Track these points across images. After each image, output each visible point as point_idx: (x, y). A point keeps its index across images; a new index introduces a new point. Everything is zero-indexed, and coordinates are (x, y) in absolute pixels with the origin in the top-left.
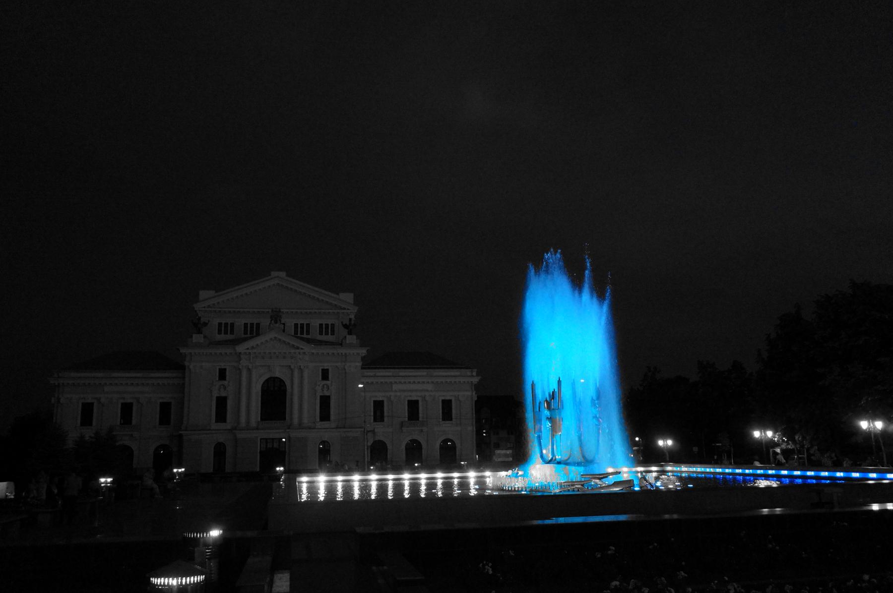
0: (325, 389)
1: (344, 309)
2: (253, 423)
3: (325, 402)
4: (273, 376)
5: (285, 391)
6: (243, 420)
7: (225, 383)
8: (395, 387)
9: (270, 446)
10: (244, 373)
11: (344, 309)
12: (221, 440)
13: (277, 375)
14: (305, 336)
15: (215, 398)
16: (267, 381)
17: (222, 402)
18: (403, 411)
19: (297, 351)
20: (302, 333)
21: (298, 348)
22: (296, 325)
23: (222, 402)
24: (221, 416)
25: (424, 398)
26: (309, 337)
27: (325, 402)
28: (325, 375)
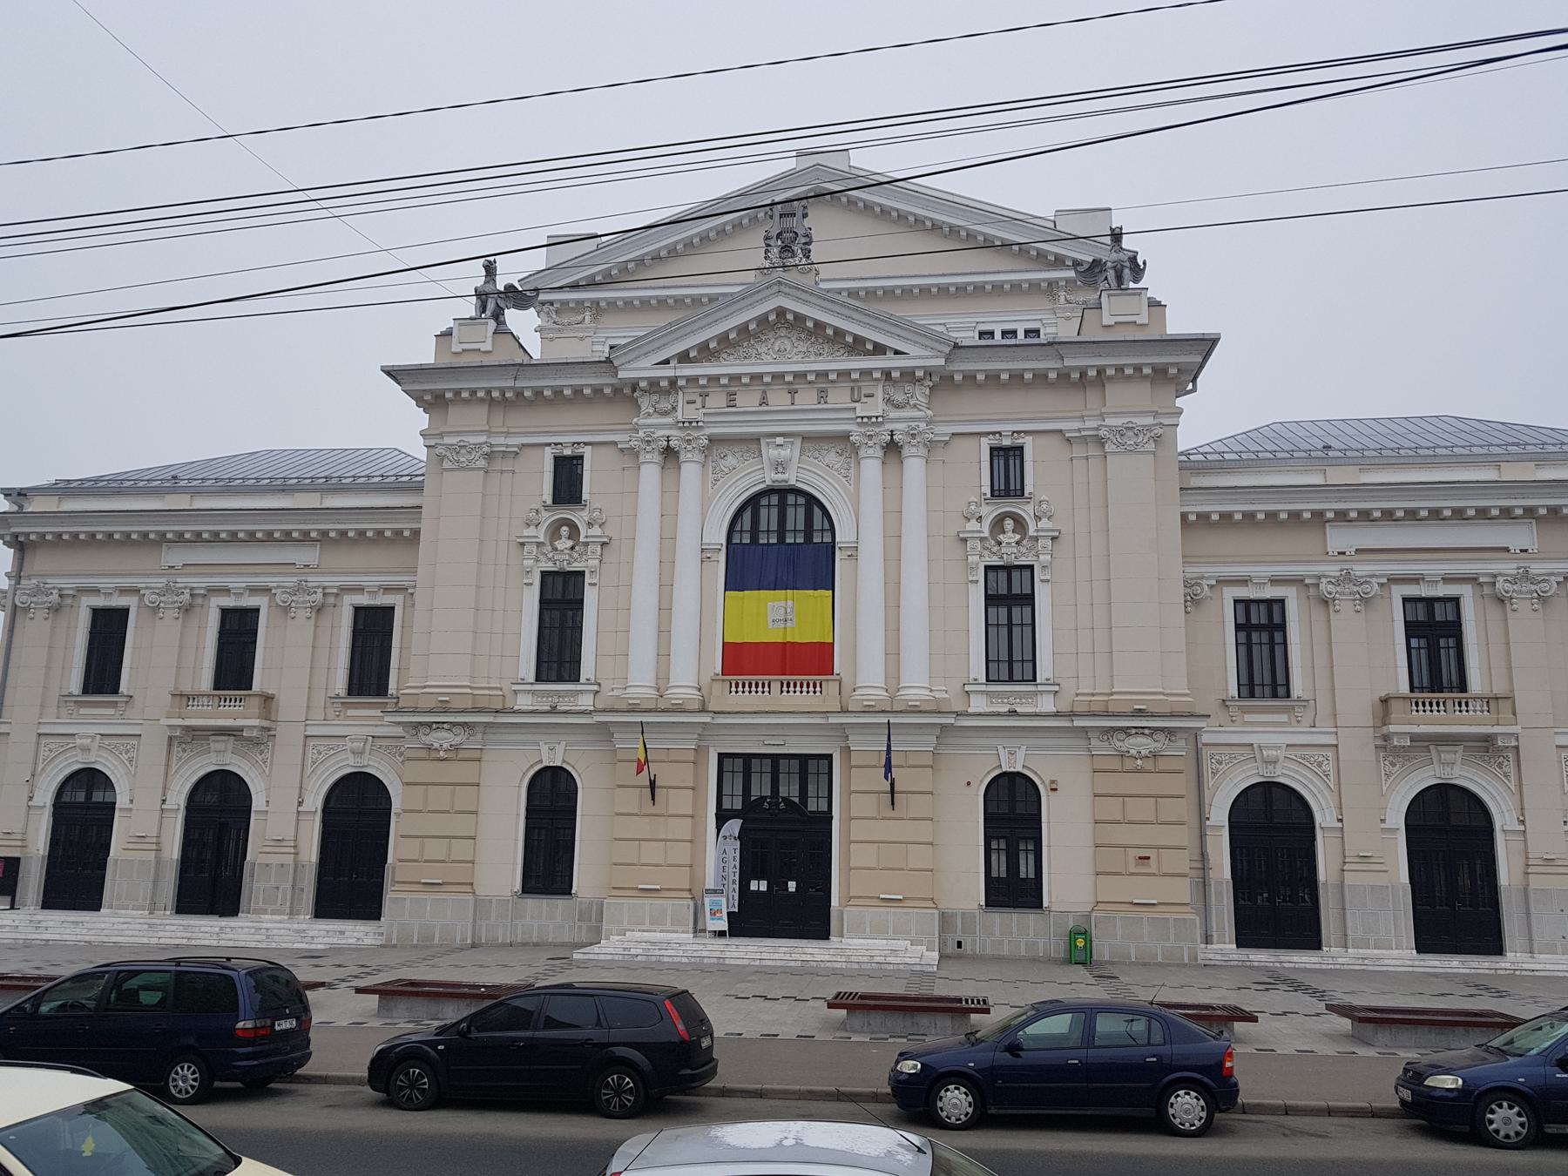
4: (770, 478)
7: (579, 517)
8: (1340, 539)
9: (761, 788)
13: (791, 478)
16: (753, 503)
21: (879, 349)
23: (562, 601)
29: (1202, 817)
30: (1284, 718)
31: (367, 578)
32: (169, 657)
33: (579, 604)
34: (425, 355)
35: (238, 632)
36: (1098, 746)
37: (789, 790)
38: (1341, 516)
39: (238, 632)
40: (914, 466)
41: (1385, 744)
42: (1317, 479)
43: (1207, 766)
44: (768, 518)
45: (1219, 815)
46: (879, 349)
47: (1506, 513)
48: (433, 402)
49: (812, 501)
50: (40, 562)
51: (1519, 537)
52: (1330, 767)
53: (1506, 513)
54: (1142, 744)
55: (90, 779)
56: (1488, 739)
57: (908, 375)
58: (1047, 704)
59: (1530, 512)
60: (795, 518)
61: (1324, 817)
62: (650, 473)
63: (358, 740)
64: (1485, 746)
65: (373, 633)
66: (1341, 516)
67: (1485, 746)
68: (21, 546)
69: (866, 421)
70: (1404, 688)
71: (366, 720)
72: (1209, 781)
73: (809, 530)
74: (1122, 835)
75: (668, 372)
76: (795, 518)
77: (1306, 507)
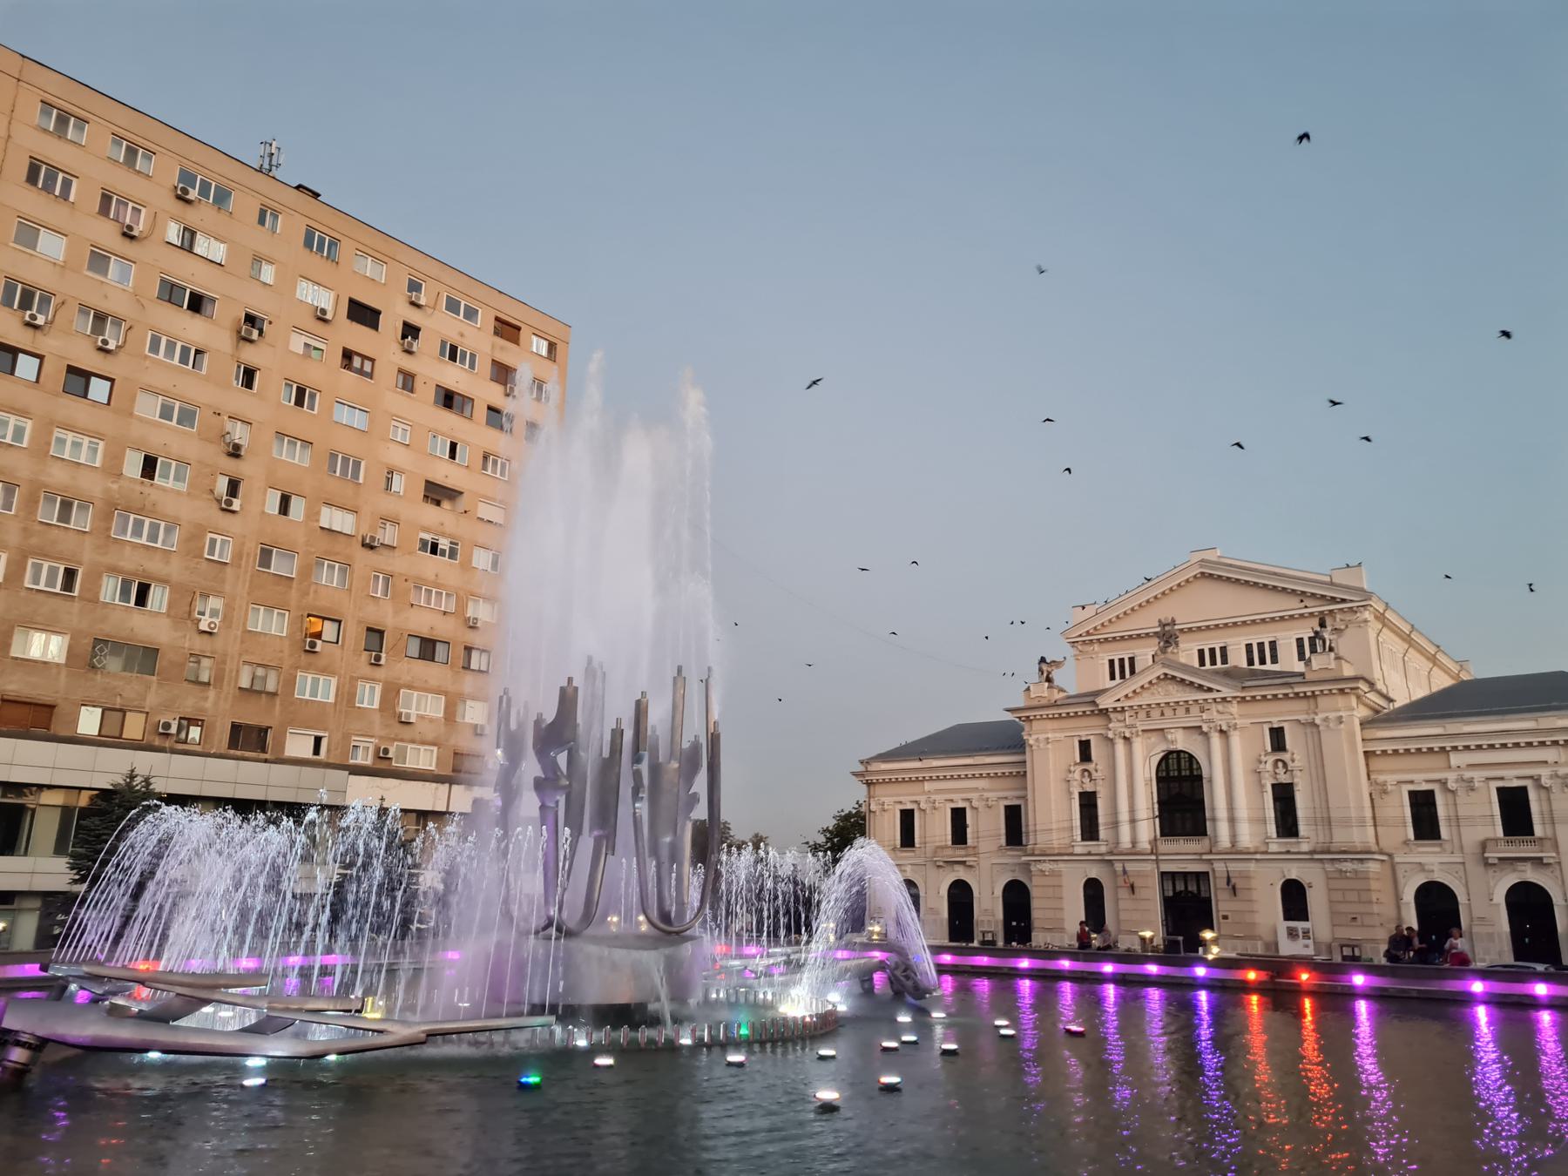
0: (1281, 770)
1: (1343, 601)
2: (1144, 844)
3: (1284, 796)
4: (1172, 747)
5: (1200, 778)
7: (1090, 767)
9: (1180, 887)
10: (1120, 747)
11: (1343, 601)
13: (1180, 748)
14: (1269, 666)
15: (1076, 796)
17: (1088, 802)
21: (1210, 690)
22: (1249, 647)
23: (1088, 802)
24: (1090, 829)
25: (1536, 780)
27: (1284, 796)
28: (1278, 737)
29: (1398, 898)
30: (1437, 849)
33: (1095, 806)
35: (958, 816)
36: (1329, 867)
37: (1192, 888)
38: (1455, 748)
39: (958, 816)
40: (1236, 739)
41: (1487, 864)
42: (1439, 731)
43: (1400, 874)
45: (1409, 896)
46: (1210, 690)
47: (1542, 744)
49: (1191, 757)
50: (878, 790)
51: (1549, 754)
52: (1461, 873)
53: (1542, 744)
54: (1348, 866)
56: (1541, 859)
57: (1224, 699)
58: (1305, 847)
59: (1555, 743)
61: (1462, 898)
62: (1120, 747)
64: (1538, 862)
65: (1014, 817)
66: (1455, 748)
68: (869, 784)
69: (1210, 721)
70: (1500, 832)
72: (1401, 880)
73: (1191, 769)
74: (1343, 908)
75: (1118, 705)
77: (1436, 745)
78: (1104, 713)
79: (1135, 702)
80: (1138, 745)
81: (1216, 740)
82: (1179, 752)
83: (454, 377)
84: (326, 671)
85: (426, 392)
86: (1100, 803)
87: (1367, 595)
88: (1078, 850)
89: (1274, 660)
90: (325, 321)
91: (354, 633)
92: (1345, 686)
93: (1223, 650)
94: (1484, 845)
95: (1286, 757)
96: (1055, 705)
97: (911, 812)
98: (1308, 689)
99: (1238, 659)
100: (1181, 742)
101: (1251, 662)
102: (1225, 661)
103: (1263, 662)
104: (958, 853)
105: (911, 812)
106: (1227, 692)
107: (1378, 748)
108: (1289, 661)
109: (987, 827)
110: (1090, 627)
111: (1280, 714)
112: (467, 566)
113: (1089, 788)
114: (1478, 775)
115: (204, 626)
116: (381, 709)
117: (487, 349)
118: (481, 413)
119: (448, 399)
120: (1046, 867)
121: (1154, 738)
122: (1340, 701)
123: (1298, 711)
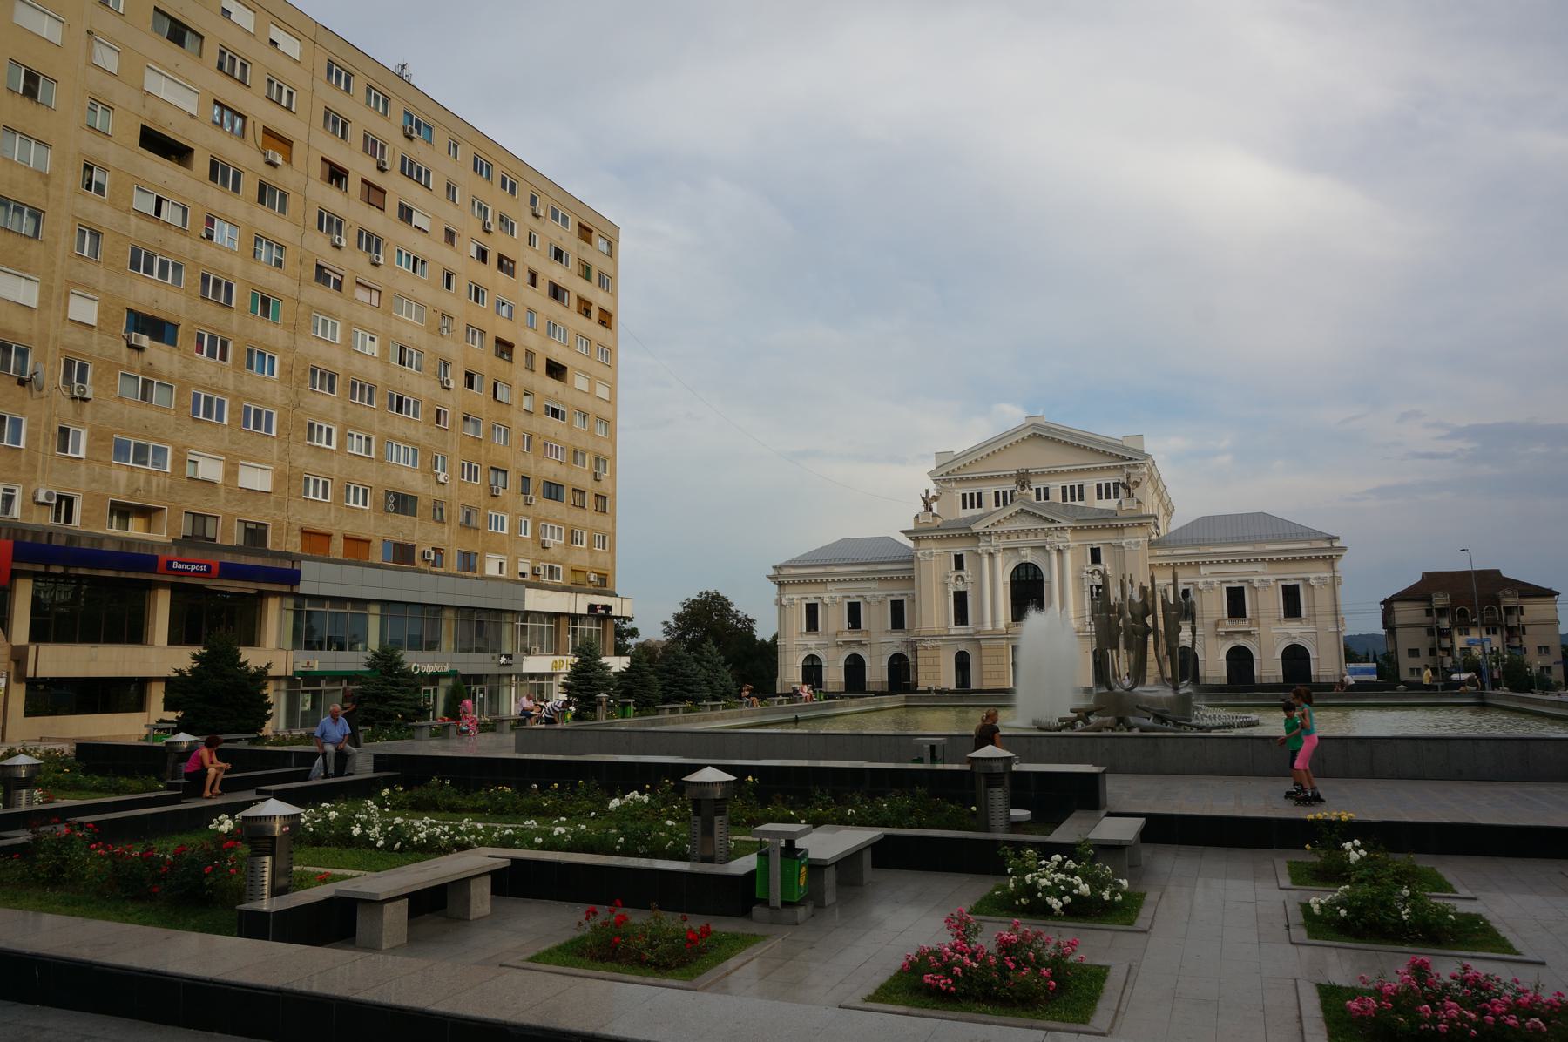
2: (1001, 625)
6: (988, 626)
8: (1203, 570)
12: (962, 649)
13: (1029, 560)
16: (1017, 568)
17: (961, 599)
18: (1221, 606)
19: (1053, 526)
20: (1073, 499)
23: (961, 599)
24: (961, 617)
26: (1081, 504)
28: (1096, 556)
31: (897, 593)
32: (834, 619)
34: (912, 527)
35: (854, 611)
39: (854, 611)
40: (1068, 555)
44: (1023, 572)
48: (916, 540)
49: (1035, 567)
51: (1259, 568)
55: (812, 657)
60: (1031, 571)
63: (894, 643)
64: (1248, 634)
65: (897, 609)
67: (1248, 634)
68: (780, 584)
71: (898, 637)
76: (1031, 571)
78: (976, 536)
79: (999, 529)
80: (999, 559)
81: (1054, 556)
82: (1027, 564)
83: (558, 273)
84: (504, 510)
85: (543, 286)
86: (969, 600)
87: (1148, 456)
88: (952, 632)
89: (1081, 498)
90: (488, 232)
91: (514, 480)
92: (1143, 521)
93: (1046, 490)
94: (1217, 625)
95: (1101, 568)
96: (938, 529)
97: (816, 605)
98: (1119, 523)
99: (1056, 496)
100: (1029, 558)
101: (1064, 499)
102: (1047, 498)
103: (1073, 499)
104: (854, 637)
105: (816, 605)
106: (1064, 524)
107: (1157, 562)
108: (1092, 501)
109: (876, 618)
110: (949, 469)
111: (1096, 540)
112: (570, 426)
113: (961, 588)
114: (1216, 580)
115: (441, 479)
116: (532, 538)
117: (574, 249)
118: (574, 303)
119: (556, 292)
120: (929, 644)
121: (1009, 554)
122: (1139, 532)
123: (1110, 537)
